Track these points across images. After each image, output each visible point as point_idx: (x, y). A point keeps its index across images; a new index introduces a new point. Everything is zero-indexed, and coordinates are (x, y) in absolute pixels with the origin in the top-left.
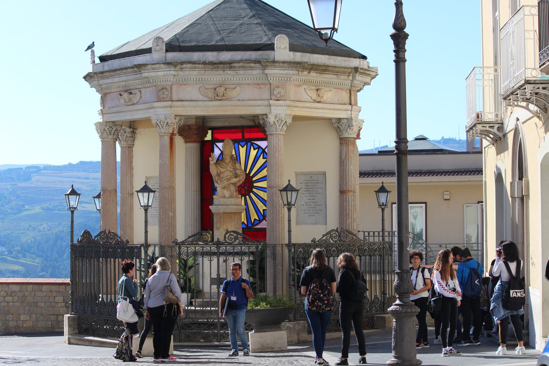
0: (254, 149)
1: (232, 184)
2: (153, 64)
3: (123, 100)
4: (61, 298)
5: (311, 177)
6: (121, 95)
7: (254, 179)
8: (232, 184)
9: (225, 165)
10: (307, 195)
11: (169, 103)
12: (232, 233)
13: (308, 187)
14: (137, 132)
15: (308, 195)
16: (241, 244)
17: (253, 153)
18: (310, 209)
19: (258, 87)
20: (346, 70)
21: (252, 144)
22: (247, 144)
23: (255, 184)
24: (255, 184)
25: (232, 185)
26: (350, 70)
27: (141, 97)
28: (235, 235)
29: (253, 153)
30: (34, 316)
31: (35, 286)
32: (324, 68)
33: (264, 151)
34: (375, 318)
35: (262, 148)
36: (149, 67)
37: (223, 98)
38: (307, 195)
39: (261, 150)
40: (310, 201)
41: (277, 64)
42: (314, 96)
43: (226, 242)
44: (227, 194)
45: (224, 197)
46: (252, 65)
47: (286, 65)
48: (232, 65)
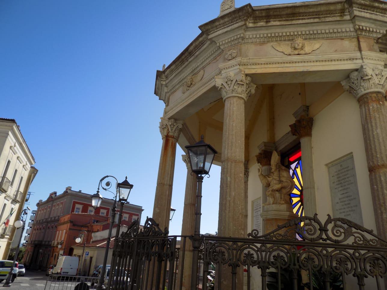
1: (277, 191)
5: (341, 166)
8: (277, 191)
13: (340, 179)
15: (340, 189)
19: (215, 61)
20: (332, 8)
25: (277, 192)
26: (339, 7)
32: (289, 11)
38: (340, 189)
41: (217, 23)
42: (288, 50)
46: (201, 39)
47: (226, 20)
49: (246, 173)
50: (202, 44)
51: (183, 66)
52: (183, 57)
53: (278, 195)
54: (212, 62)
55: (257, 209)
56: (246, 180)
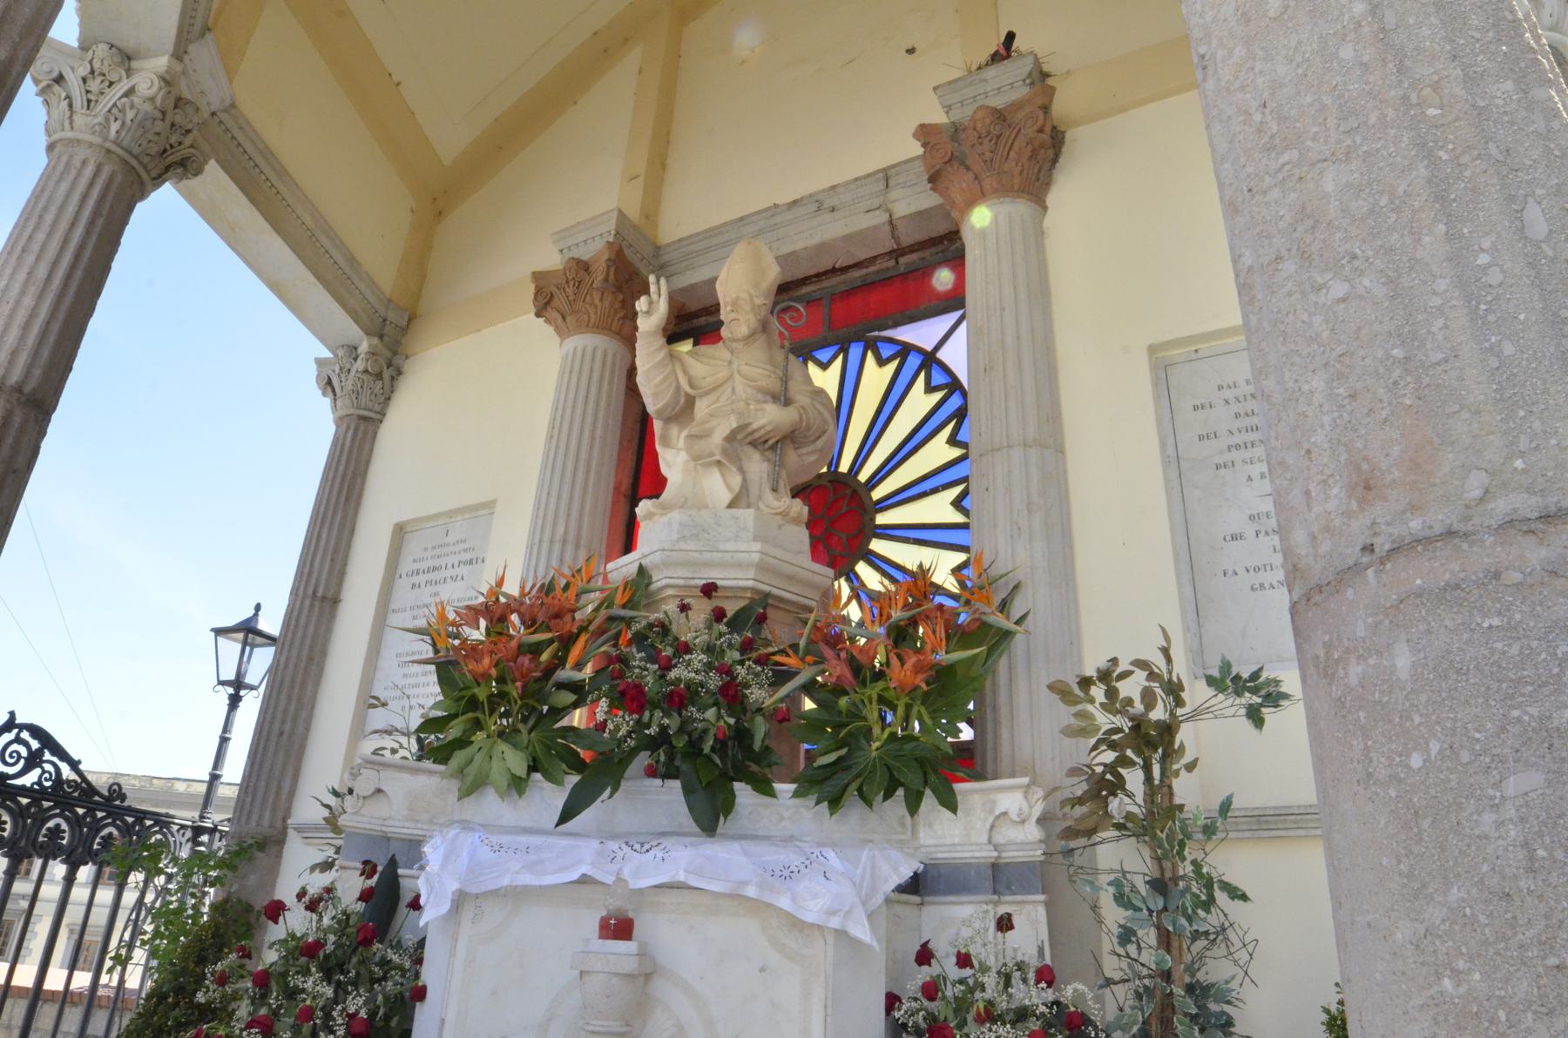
0: (882, 362)
7: (877, 494)
9: (726, 355)
14: (408, 367)
17: (876, 378)
21: (871, 345)
22: (845, 350)
23: (881, 519)
25: (756, 456)
29: (876, 378)
33: (930, 360)
35: (920, 350)
39: (914, 361)
44: (717, 487)
49: (386, 375)
53: (758, 466)
55: (435, 569)
56: (377, 408)
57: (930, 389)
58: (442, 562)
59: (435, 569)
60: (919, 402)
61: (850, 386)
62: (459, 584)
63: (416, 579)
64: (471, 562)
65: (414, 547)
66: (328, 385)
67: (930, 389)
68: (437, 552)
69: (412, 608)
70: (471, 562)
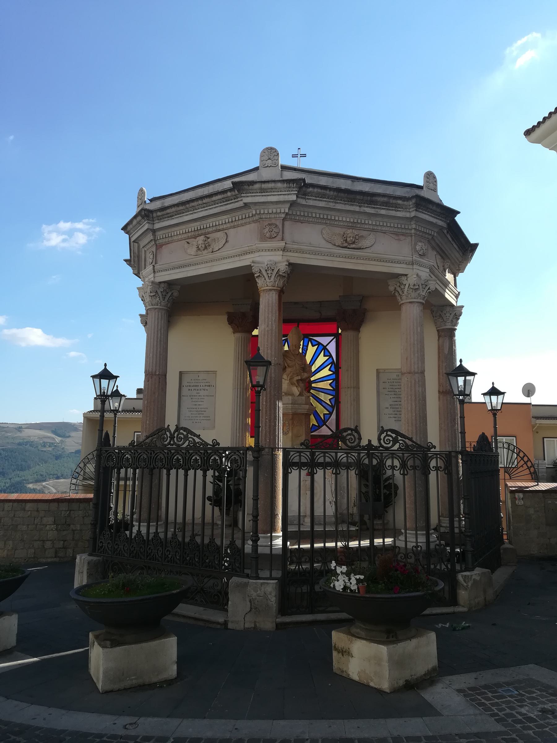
0: (313, 346)
2: (264, 182)
3: (195, 249)
4: (51, 520)
6: (188, 243)
10: (392, 396)
11: (282, 244)
12: (389, 433)
15: (394, 396)
16: (402, 450)
18: (396, 412)
19: (396, 238)
21: (310, 340)
23: (313, 385)
24: (313, 385)
27: (226, 242)
28: (394, 435)
29: (311, 350)
30: (11, 542)
31: (15, 504)
33: (325, 348)
34: (502, 551)
36: (257, 186)
37: (353, 246)
38: (394, 396)
39: (321, 347)
40: (396, 403)
41: (431, 206)
43: (381, 446)
45: (292, 395)
46: (400, 202)
47: (438, 210)
48: (374, 198)
50: (396, 207)
51: (348, 208)
52: (358, 197)
54: (390, 235)
55: (196, 386)
57: (324, 356)
58: (199, 384)
59: (196, 386)
60: (322, 359)
61: (305, 349)
62: (206, 391)
63: (190, 388)
64: (209, 386)
65: (186, 379)
66: (145, 323)
67: (324, 356)
68: (196, 381)
69: (190, 396)
70: (209, 386)
